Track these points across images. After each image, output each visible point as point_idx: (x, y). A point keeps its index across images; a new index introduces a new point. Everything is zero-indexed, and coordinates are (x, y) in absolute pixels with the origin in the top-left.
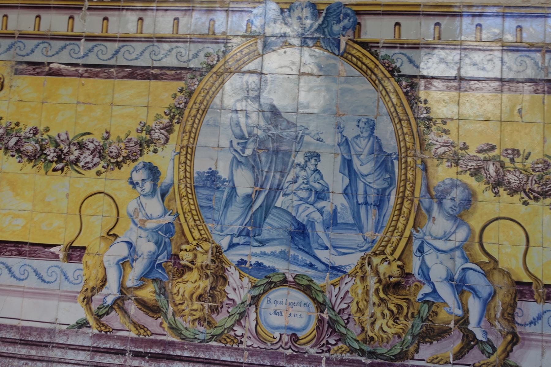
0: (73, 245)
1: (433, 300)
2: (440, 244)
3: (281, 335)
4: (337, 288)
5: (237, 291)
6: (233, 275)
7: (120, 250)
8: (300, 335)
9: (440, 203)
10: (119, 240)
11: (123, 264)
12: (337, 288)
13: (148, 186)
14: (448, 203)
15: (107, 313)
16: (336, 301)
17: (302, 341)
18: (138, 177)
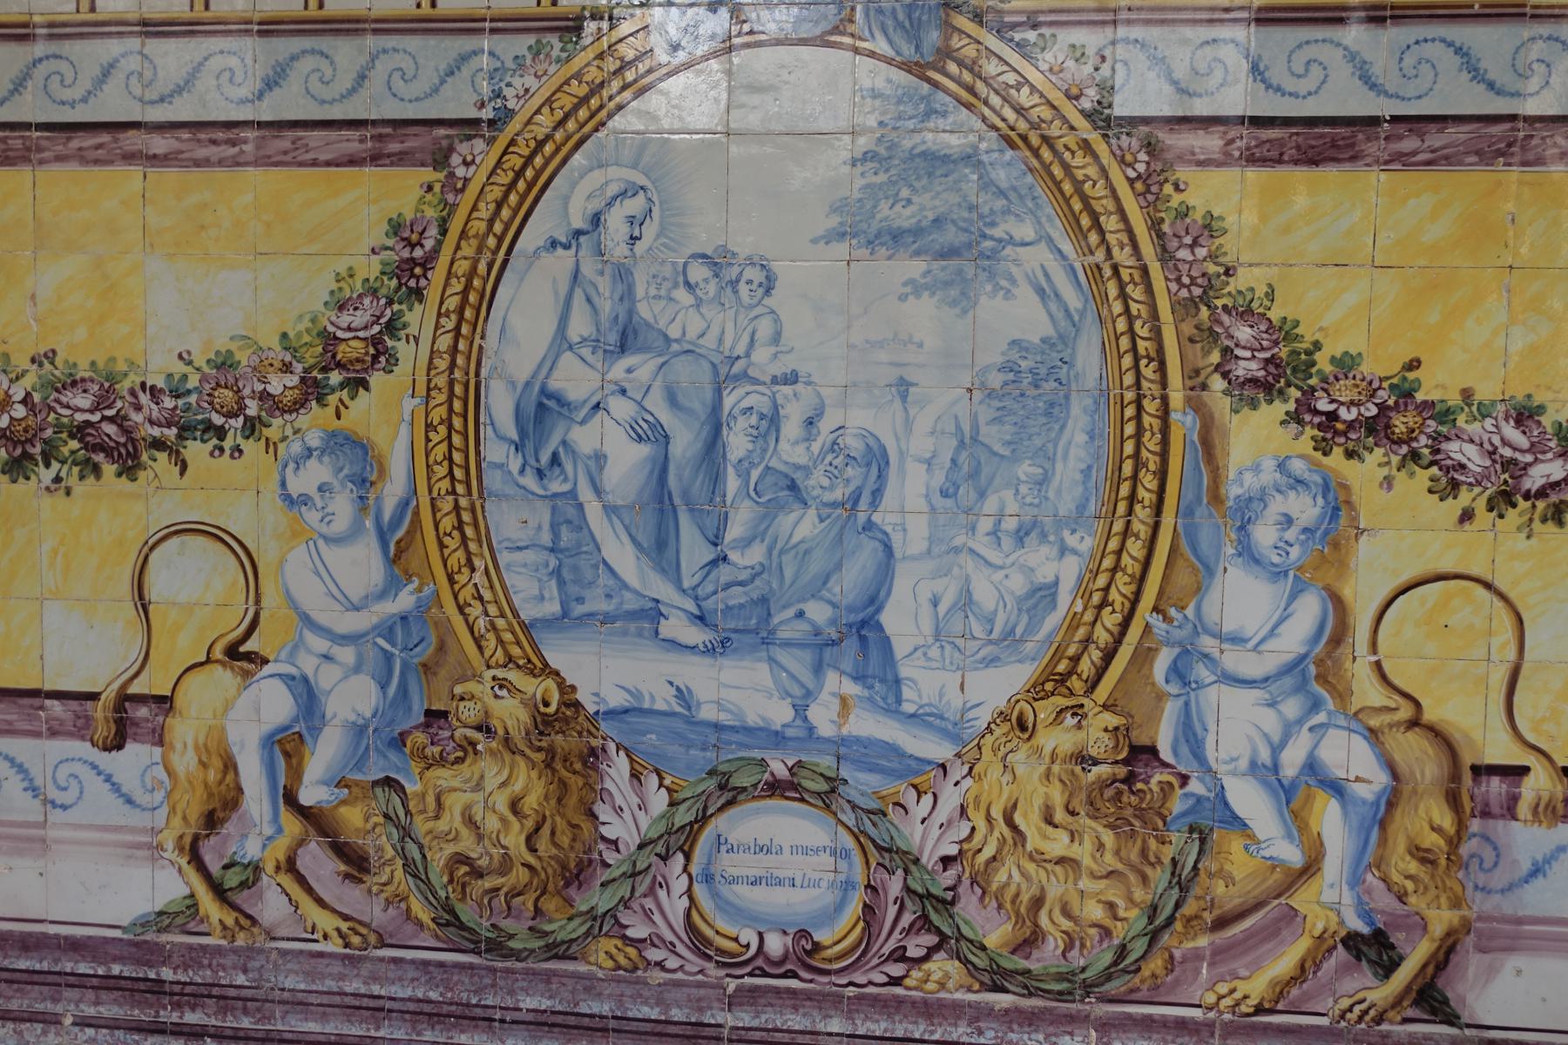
0: (134, 689)
1: (1214, 822)
2: (1233, 660)
3: (761, 935)
4: (927, 800)
5: (627, 815)
7: (271, 703)
8: (822, 936)
10: (267, 670)
11: (288, 747)
12: (927, 800)
13: (342, 506)
14: (1264, 535)
16: (924, 837)
17: (829, 953)
18: (305, 481)
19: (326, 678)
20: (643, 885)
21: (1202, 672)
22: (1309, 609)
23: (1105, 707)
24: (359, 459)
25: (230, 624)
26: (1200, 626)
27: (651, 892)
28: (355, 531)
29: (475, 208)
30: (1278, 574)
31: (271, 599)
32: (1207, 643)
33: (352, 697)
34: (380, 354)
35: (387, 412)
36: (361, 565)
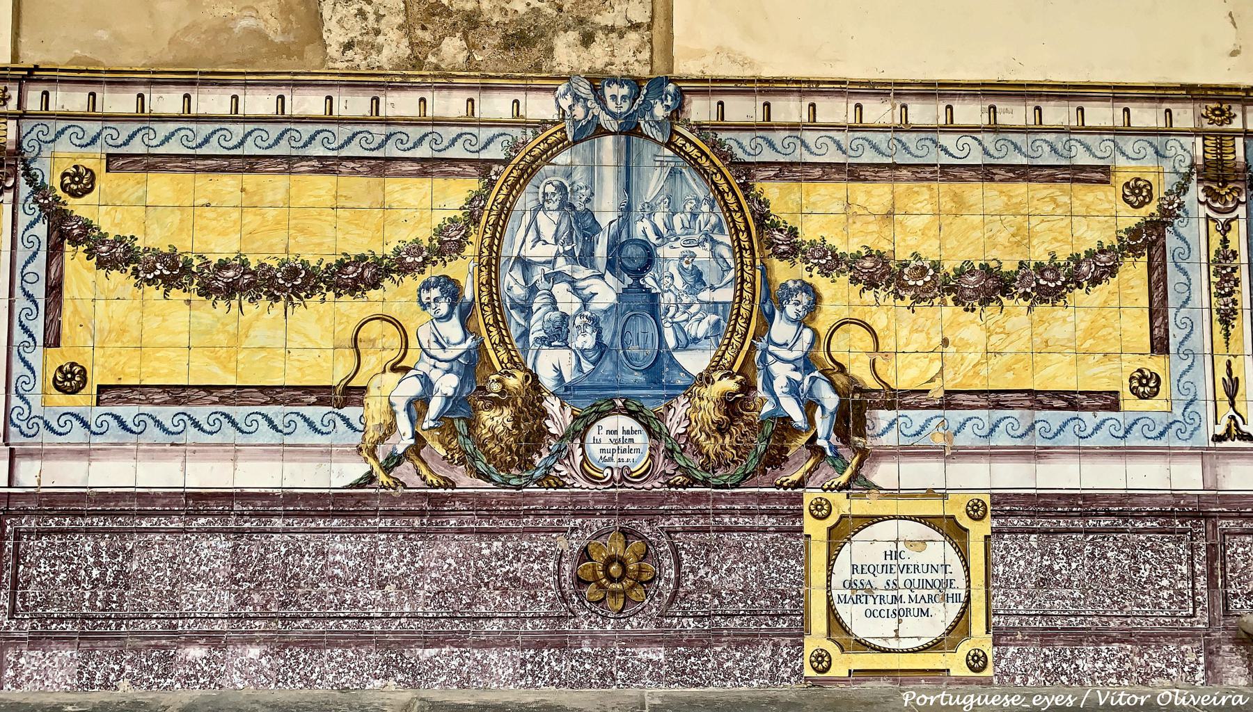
2: (783, 353)
6: (552, 405)
9: (783, 309)
10: (412, 372)
15: (398, 464)
19: (434, 375)
20: (564, 454)
21: (770, 358)
22: (807, 335)
23: (739, 373)
24: (451, 289)
25: (391, 356)
26: (770, 341)
27: (568, 457)
28: (448, 317)
29: (498, 194)
30: (794, 321)
31: (413, 343)
32: (771, 348)
33: (447, 384)
34: (460, 246)
35: (463, 270)
36: (452, 330)
